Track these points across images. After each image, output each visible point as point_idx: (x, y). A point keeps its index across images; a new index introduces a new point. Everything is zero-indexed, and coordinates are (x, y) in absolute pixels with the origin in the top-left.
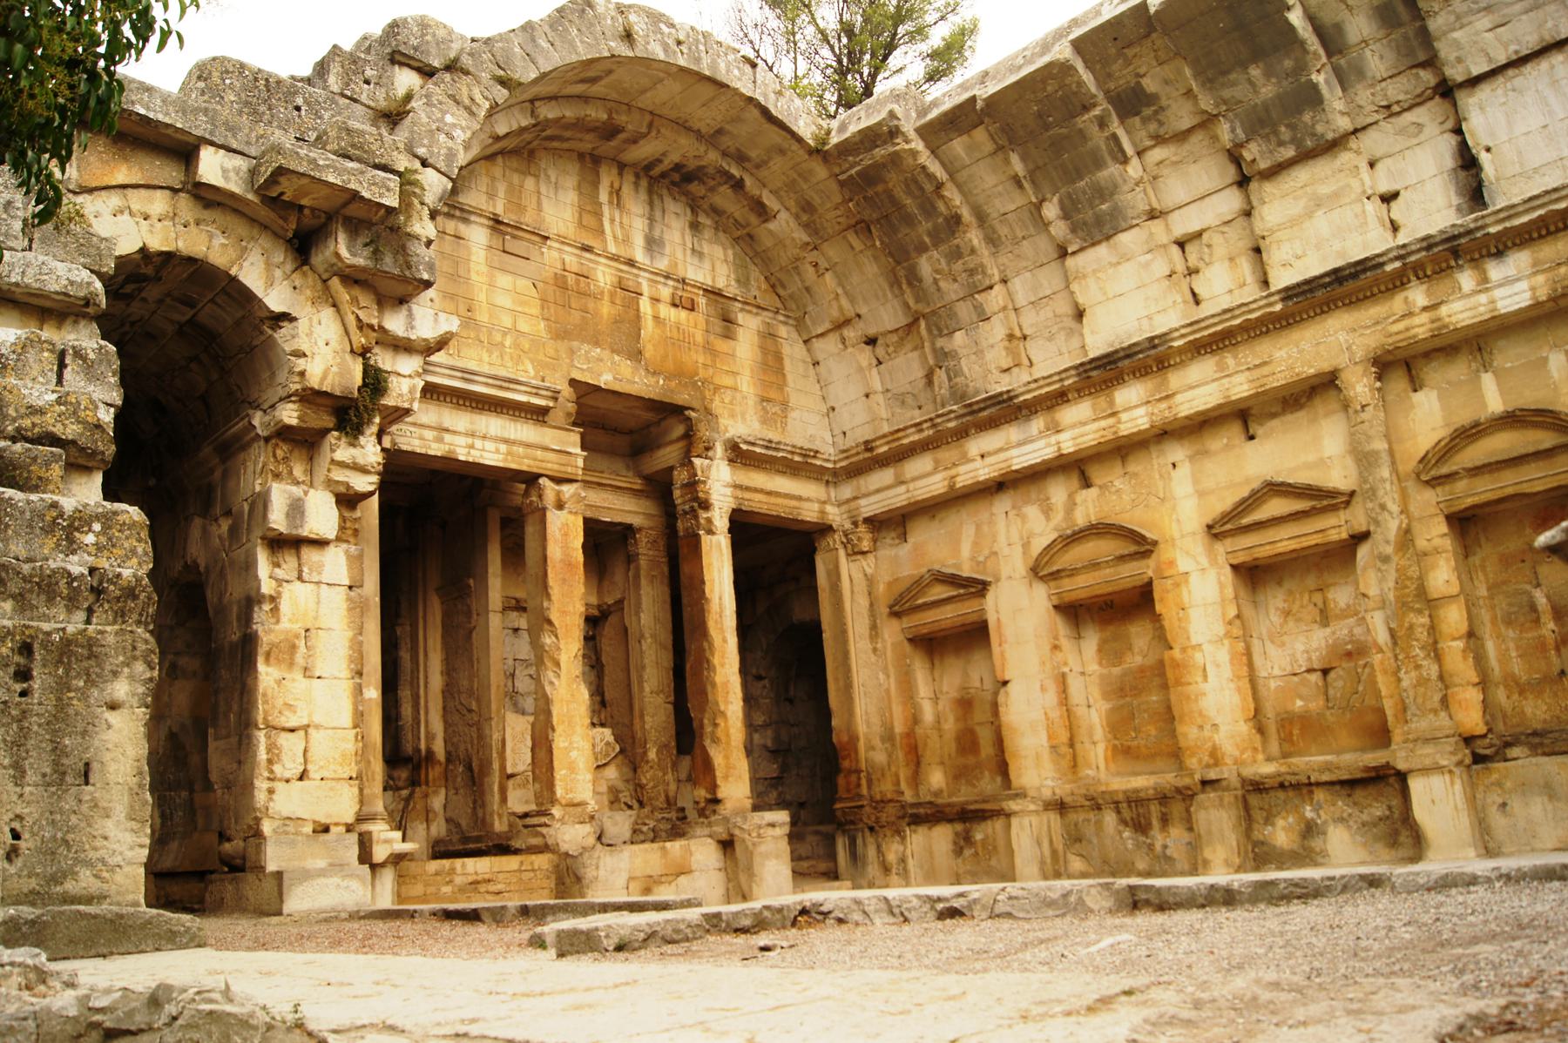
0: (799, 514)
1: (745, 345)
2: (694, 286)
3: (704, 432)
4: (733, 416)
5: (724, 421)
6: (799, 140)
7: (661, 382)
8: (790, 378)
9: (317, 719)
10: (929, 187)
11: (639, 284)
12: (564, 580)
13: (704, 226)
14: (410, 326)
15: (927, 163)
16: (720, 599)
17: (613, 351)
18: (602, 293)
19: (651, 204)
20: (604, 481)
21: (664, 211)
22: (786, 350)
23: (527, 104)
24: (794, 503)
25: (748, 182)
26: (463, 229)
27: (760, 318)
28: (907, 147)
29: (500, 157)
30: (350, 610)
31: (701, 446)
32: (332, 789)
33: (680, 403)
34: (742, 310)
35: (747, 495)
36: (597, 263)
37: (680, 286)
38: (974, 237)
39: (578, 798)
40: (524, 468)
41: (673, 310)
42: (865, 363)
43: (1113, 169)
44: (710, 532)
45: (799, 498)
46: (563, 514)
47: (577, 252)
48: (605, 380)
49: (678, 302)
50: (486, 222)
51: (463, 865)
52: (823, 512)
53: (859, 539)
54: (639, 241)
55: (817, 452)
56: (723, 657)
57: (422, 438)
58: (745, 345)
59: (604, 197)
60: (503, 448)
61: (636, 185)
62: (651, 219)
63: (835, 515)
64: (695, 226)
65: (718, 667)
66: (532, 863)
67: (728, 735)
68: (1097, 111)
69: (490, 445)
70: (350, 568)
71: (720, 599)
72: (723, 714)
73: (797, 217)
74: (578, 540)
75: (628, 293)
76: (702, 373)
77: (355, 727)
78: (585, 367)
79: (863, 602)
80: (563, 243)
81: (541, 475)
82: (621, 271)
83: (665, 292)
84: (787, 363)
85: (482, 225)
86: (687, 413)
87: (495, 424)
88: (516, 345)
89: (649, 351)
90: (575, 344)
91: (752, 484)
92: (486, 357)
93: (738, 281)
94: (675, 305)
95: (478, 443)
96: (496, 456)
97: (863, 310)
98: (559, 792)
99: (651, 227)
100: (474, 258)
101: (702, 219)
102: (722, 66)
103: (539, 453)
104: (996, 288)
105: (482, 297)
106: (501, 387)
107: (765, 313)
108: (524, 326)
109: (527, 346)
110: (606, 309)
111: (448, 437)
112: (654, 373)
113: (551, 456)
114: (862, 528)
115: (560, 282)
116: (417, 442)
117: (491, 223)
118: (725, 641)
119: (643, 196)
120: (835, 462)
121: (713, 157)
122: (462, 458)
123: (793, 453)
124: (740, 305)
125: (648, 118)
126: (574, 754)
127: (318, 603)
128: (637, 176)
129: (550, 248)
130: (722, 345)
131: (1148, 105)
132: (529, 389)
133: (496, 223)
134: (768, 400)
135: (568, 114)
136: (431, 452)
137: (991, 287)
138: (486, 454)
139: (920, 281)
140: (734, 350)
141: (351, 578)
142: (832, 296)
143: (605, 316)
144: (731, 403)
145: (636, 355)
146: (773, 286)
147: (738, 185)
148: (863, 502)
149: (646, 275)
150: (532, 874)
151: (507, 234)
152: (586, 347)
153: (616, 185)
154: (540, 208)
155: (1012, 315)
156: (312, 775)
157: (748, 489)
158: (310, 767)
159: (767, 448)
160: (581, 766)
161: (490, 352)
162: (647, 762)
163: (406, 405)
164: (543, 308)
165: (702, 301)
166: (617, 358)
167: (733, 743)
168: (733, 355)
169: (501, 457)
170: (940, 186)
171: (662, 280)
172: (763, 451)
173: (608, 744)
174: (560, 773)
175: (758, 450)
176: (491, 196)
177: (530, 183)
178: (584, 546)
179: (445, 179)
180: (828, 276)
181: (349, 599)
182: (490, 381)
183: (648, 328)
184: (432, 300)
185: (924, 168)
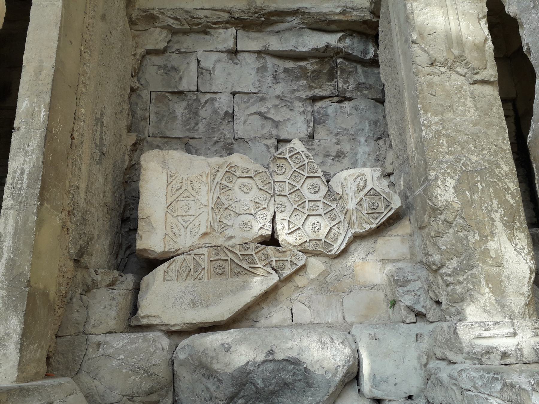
162: (435, 211)
173: (373, 193)
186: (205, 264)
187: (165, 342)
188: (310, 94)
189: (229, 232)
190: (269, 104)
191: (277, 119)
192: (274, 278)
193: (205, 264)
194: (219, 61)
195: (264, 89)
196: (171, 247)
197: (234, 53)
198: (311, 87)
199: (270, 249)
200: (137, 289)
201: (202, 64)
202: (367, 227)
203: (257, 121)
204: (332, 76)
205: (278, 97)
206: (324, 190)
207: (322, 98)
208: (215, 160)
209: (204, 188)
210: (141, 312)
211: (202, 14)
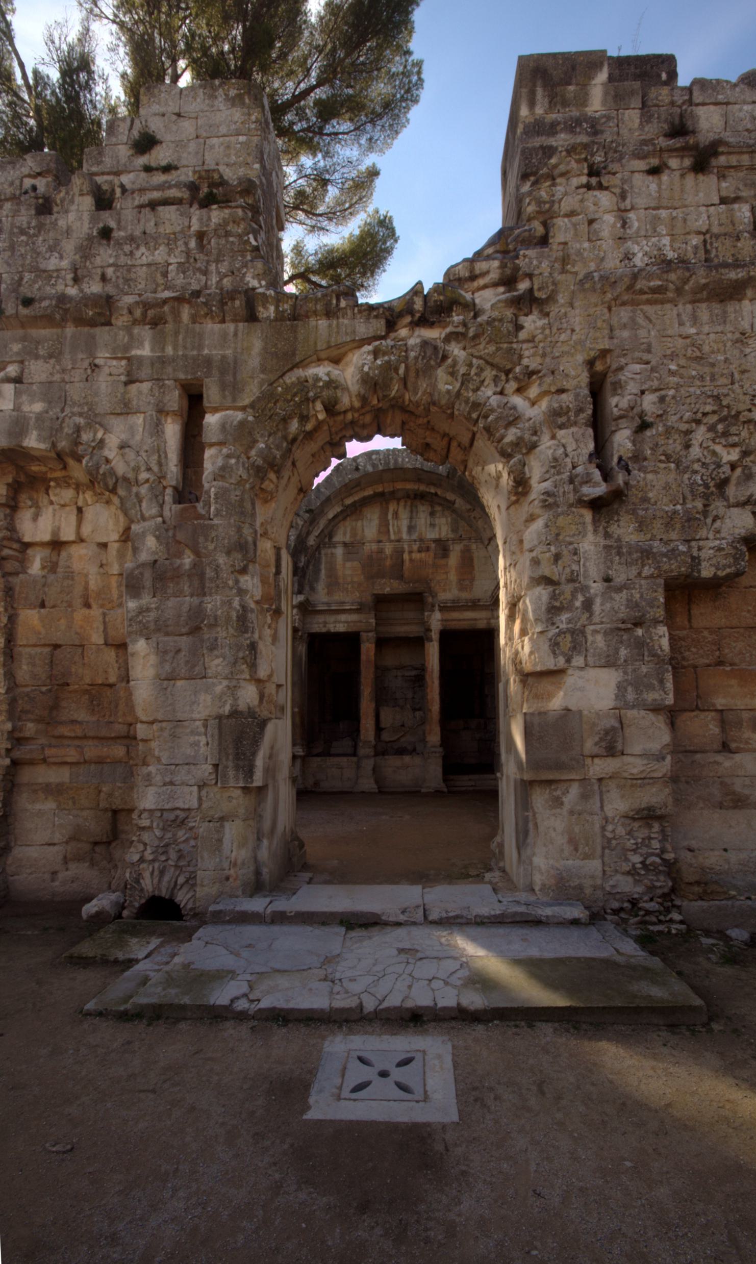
11: (403, 548)
19: (411, 512)
48: (387, 590)
54: (404, 529)
62: (411, 518)
64: (432, 514)
75: (399, 553)
76: (430, 577)
83: (415, 547)
89: (407, 574)
94: (419, 551)
99: (411, 522)
101: (438, 508)
110: (388, 563)
145: (401, 577)
165: (433, 545)
183: (407, 564)
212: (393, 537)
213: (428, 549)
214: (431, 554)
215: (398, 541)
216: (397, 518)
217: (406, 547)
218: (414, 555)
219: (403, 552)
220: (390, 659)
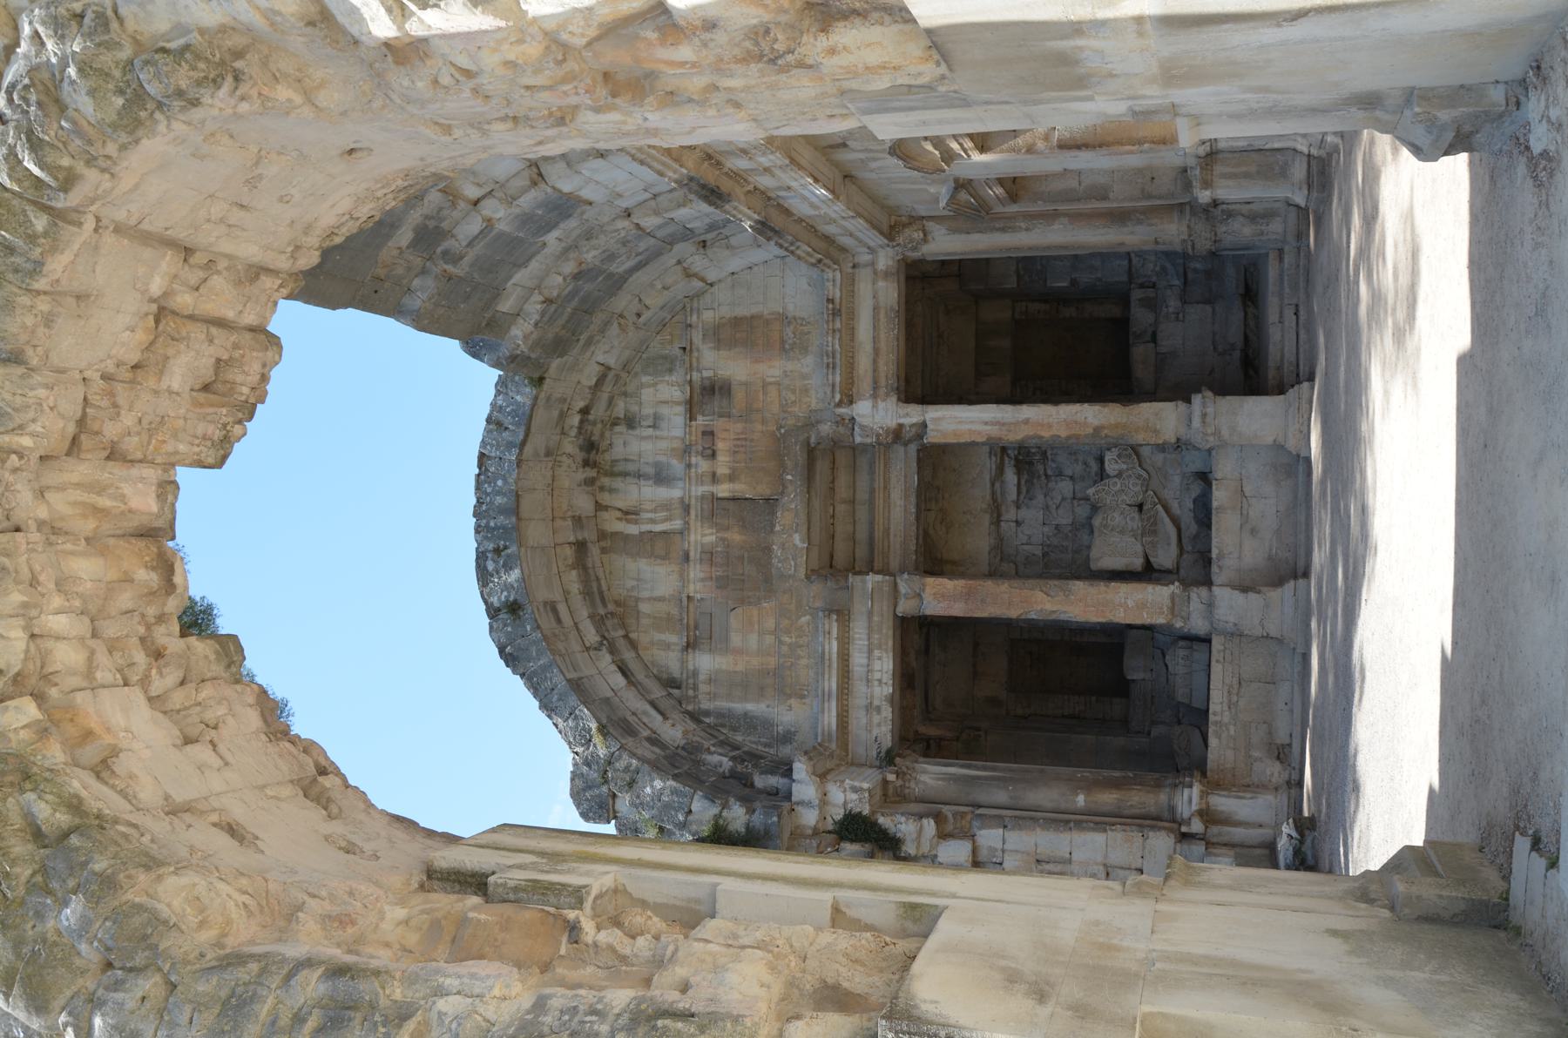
0: (891, 307)
1: (733, 367)
2: (690, 434)
3: (826, 429)
4: (805, 391)
5: (814, 400)
6: (536, 398)
7: (789, 477)
8: (754, 310)
9: (1100, 859)
10: (553, 307)
11: (703, 497)
12: (983, 601)
13: (627, 411)
14: (808, 804)
15: (532, 322)
16: (986, 423)
17: (772, 531)
18: (723, 540)
19: (625, 474)
20: (882, 485)
21: (626, 460)
22: (726, 312)
23: (591, 653)
24: (882, 316)
25: (582, 404)
26: (702, 677)
27: (701, 347)
28: (523, 346)
29: (633, 636)
30: (1020, 829)
31: (841, 429)
32: (1150, 852)
33: (805, 456)
34: (699, 371)
35: (883, 382)
36: (696, 542)
37: (694, 448)
38: (591, 256)
39: (1167, 602)
40: (891, 633)
41: (718, 453)
42: (727, 252)
43: (502, 227)
44: (924, 425)
45: (876, 309)
46: (927, 596)
47: (691, 563)
49: (709, 452)
50: (690, 657)
51: (1215, 714)
52: (886, 274)
53: (911, 241)
55: (828, 300)
56: (1042, 425)
57: (879, 725)
58: (733, 367)
59: (633, 530)
60: (877, 653)
61: (611, 491)
62: (639, 476)
63: (886, 259)
64: (631, 422)
65: (1051, 433)
66: (1219, 652)
67: (1117, 426)
68: (449, 268)
69: (877, 665)
70: (990, 827)
71: (986, 423)
72: (1097, 430)
73: (598, 341)
74: (948, 584)
75: (716, 509)
77: (1105, 831)
78: (793, 563)
79: (976, 237)
80: (688, 581)
81: (895, 615)
82: (697, 516)
83: (704, 466)
84: (742, 311)
85: (694, 659)
86: (813, 445)
87: (858, 660)
88: (788, 632)
89: (764, 490)
90: (773, 571)
91: (870, 374)
92: (804, 662)
93: (670, 371)
94: (713, 455)
95: (877, 676)
96: (885, 659)
97: (674, 261)
98: (1161, 620)
99: (646, 477)
100: (724, 667)
102: (499, 500)
103: (876, 618)
104: (636, 221)
105: (755, 662)
106: (830, 666)
107: (695, 340)
108: (770, 623)
109: (787, 621)
110: (736, 536)
111: (876, 703)
112: (784, 487)
113: (876, 607)
114: (900, 240)
115: (722, 583)
116: (883, 729)
117: (690, 650)
118: (1026, 421)
119: (618, 483)
120: (834, 270)
121: (570, 446)
122: (891, 690)
123: (834, 331)
124: (694, 374)
125: (559, 523)
126: (1130, 603)
127: (1017, 851)
128: (602, 489)
129: (696, 592)
130: (739, 395)
131: (426, 226)
132: (827, 641)
133: (690, 646)
134: (783, 342)
135: (585, 613)
136: (890, 716)
137: (637, 224)
138: (885, 670)
139: (641, 261)
140: (741, 384)
141: (998, 827)
142: (666, 292)
143: (743, 537)
144: (794, 392)
145: (770, 503)
146: (664, 326)
147: (585, 411)
148: (872, 244)
149: (693, 488)
150: (1227, 651)
151: (695, 635)
152: (775, 561)
153: (619, 514)
154: (661, 599)
155: (659, 199)
156: (1139, 866)
157: (875, 382)
158: (1133, 866)
159: (834, 368)
160: (1140, 596)
161: (799, 657)
163: (867, 795)
164: (750, 603)
165: (701, 420)
166: (778, 528)
167: (1124, 421)
168: (746, 384)
169: (885, 655)
170: (548, 301)
171: (693, 470)
172: (838, 372)
173: (1119, 456)
174: (1145, 618)
175: (838, 379)
176: (667, 646)
177: (645, 608)
178: (950, 579)
179: (696, 797)
180: (648, 302)
181: (1013, 829)
182: (826, 676)
183: (741, 488)
184: (768, 707)
185: (536, 324)
186: (1150, 539)
187: (1185, 556)
188: (1043, 477)
189: (1135, 527)
190: (1050, 503)
191: (1060, 498)
192: (1159, 507)
193: (1149, 539)
194: (1022, 532)
195: (1041, 506)
196: (1141, 554)
197: (1018, 523)
198: (1039, 477)
199: (1145, 508)
200: (1160, 571)
201: (1024, 542)
202: (1136, 460)
203: (1061, 511)
204: (1031, 463)
205: (1045, 497)
206: (1116, 480)
207: (1045, 470)
208: (1096, 534)
209: (1112, 539)
210: (1171, 567)
211: (992, 541)
212: (677, 524)
213: (709, 434)
214: (719, 424)
215: (687, 509)
216: (636, 513)
217: (706, 488)
218: (722, 470)
219: (714, 499)
220: (977, 541)
